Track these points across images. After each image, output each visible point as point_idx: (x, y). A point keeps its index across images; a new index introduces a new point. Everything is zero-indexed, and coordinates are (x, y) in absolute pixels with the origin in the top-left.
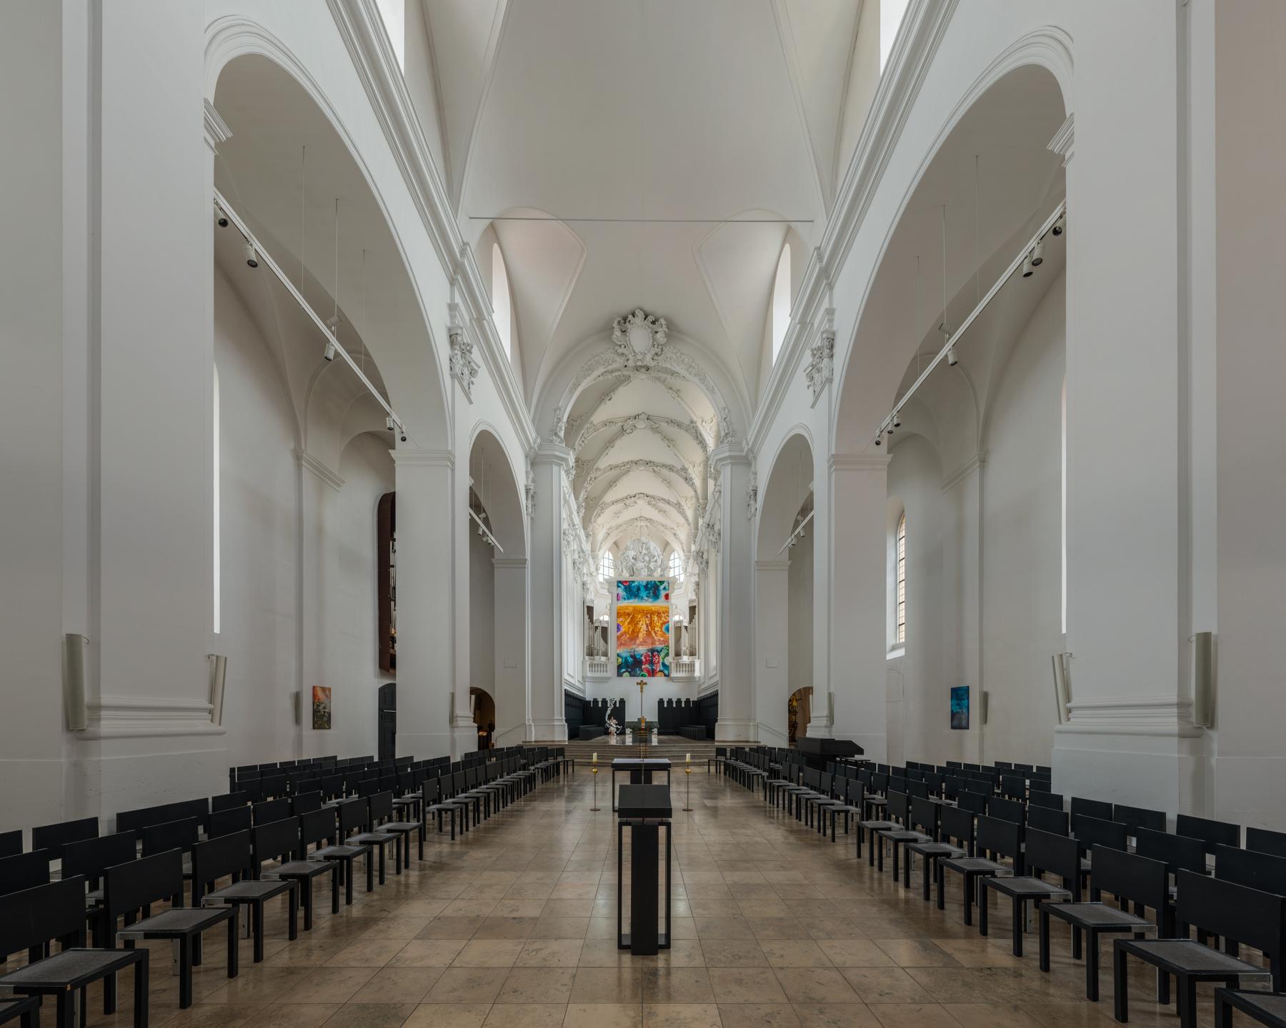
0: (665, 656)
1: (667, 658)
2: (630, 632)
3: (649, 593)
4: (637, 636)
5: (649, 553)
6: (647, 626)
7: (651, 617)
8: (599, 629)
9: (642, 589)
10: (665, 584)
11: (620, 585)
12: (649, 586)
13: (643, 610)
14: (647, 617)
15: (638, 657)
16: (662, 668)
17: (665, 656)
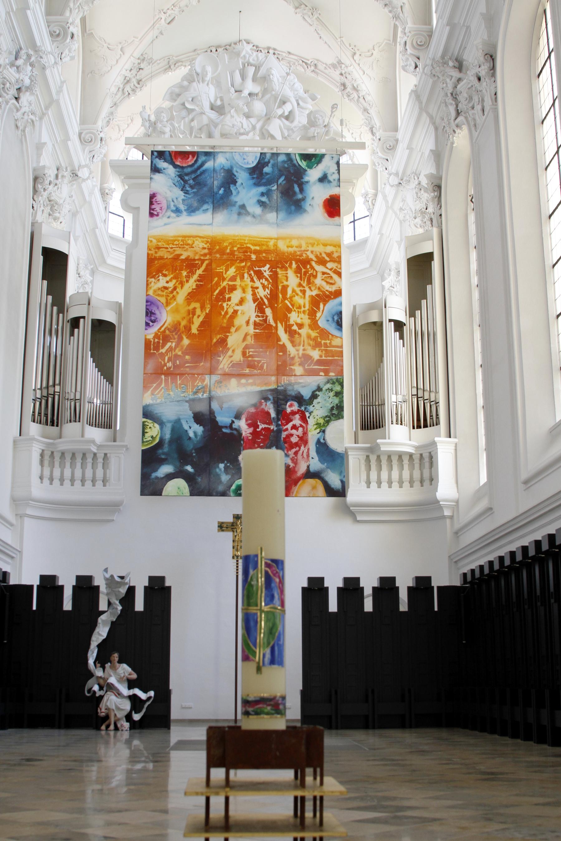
0: (328, 419)
1: (334, 425)
2: (194, 330)
3: (268, 194)
4: (223, 342)
5: (265, 91)
6: (260, 308)
7: (275, 277)
8: (85, 328)
9: (242, 177)
10: (326, 165)
11: (162, 164)
12: (267, 170)
13: (246, 250)
14: (260, 275)
15: (223, 419)
16: (315, 464)
17: (328, 419)
